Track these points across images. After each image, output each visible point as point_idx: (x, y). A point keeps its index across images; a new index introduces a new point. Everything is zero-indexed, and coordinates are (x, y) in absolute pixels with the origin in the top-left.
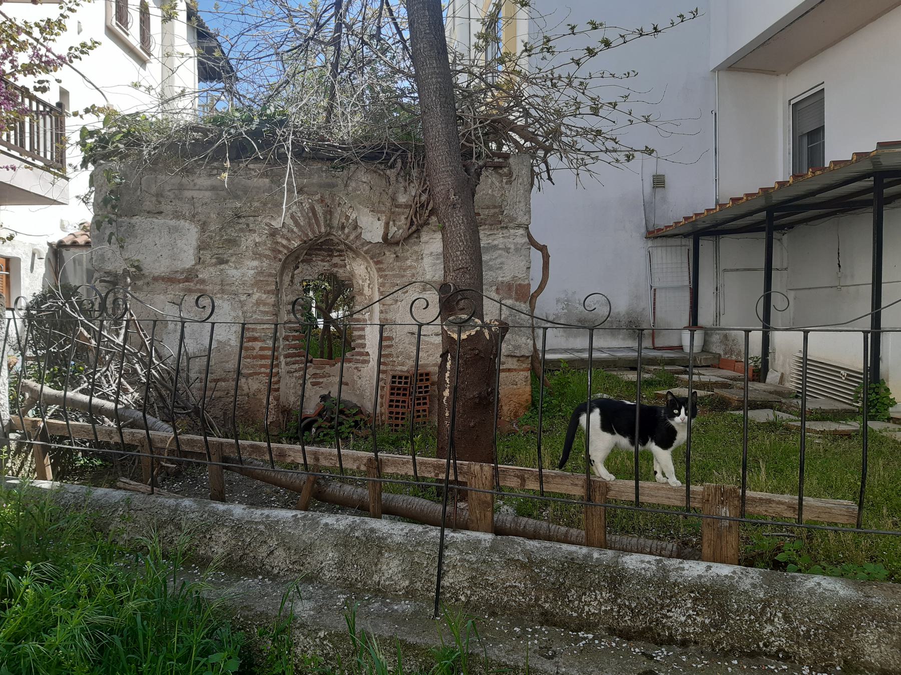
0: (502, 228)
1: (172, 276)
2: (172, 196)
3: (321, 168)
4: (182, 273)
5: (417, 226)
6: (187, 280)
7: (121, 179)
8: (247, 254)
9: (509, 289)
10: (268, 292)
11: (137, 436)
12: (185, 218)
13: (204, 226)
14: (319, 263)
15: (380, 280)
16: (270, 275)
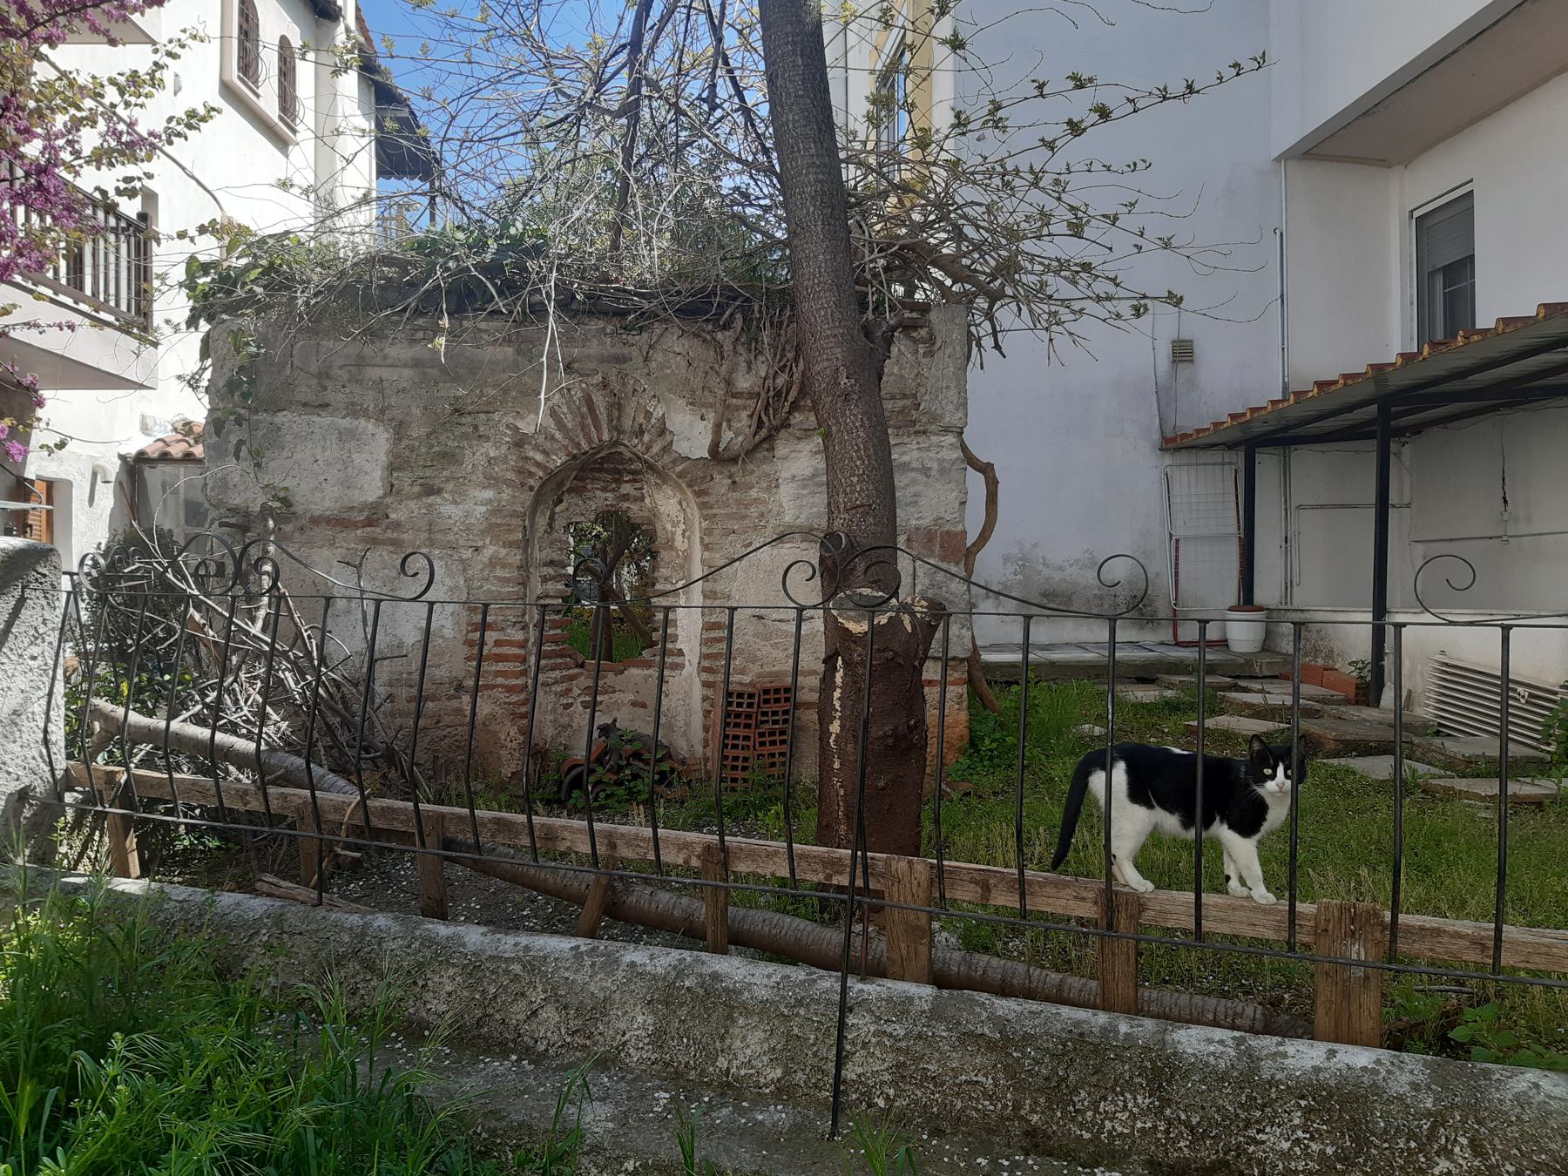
0: (917, 433)
1: (345, 516)
2: (346, 377)
3: (604, 329)
4: (361, 511)
5: (770, 430)
6: (370, 522)
7: (259, 347)
8: (474, 477)
9: (930, 541)
10: (510, 545)
11: (291, 802)
12: (368, 417)
13: (400, 430)
14: (598, 493)
15: (704, 524)
16: (514, 514)
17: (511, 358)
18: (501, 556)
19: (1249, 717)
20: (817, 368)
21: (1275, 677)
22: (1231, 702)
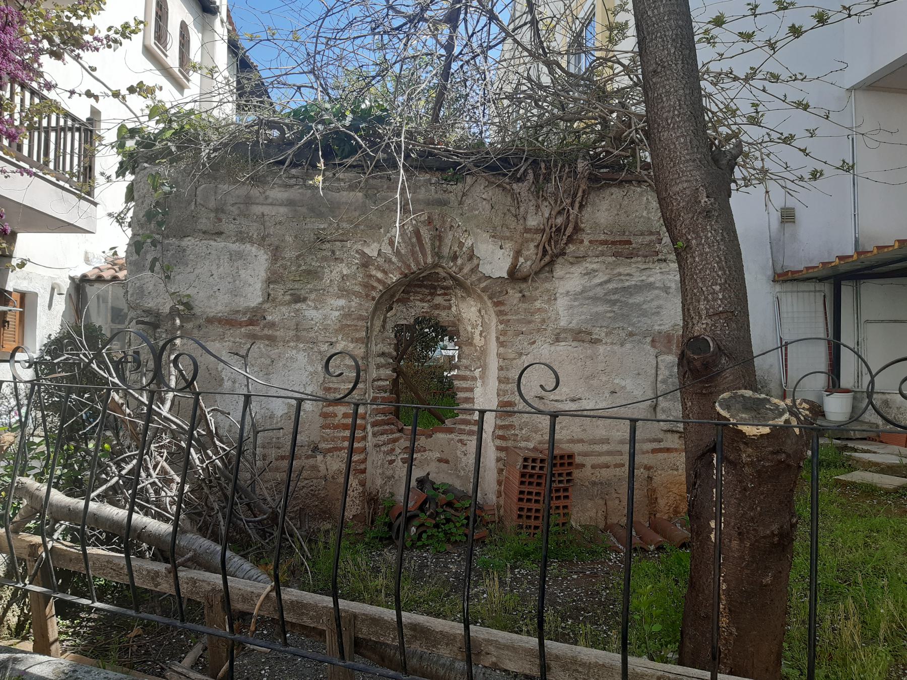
0: (658, 260)
1: (233, 317)
2: (236, 212)
3: (430, 179)
4: (245, 314)
5: (552, 257)
6: (251, 322)
7: (171, 187)
8: (331, 290)
9: (669, 342)
10: (357, 340)
11: (200, 587)
12: (251, 241)
13: (276, 253)
14: (418, 303)
15: (501, 327)
16: (360, 318)
17: (361, 201)
18: (349, 349)
19: (877, 472)
20: (676, 189)
21: (865, 439)
22: (858, 461)
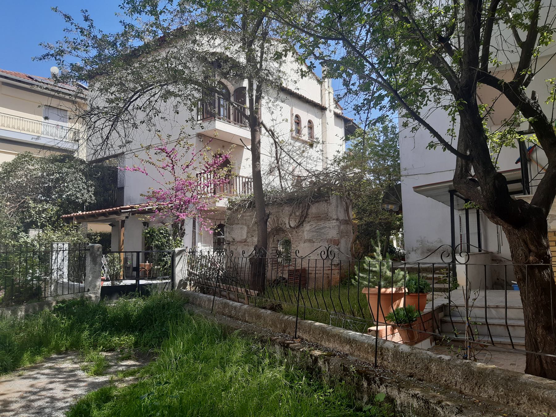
6: (245, 242)
